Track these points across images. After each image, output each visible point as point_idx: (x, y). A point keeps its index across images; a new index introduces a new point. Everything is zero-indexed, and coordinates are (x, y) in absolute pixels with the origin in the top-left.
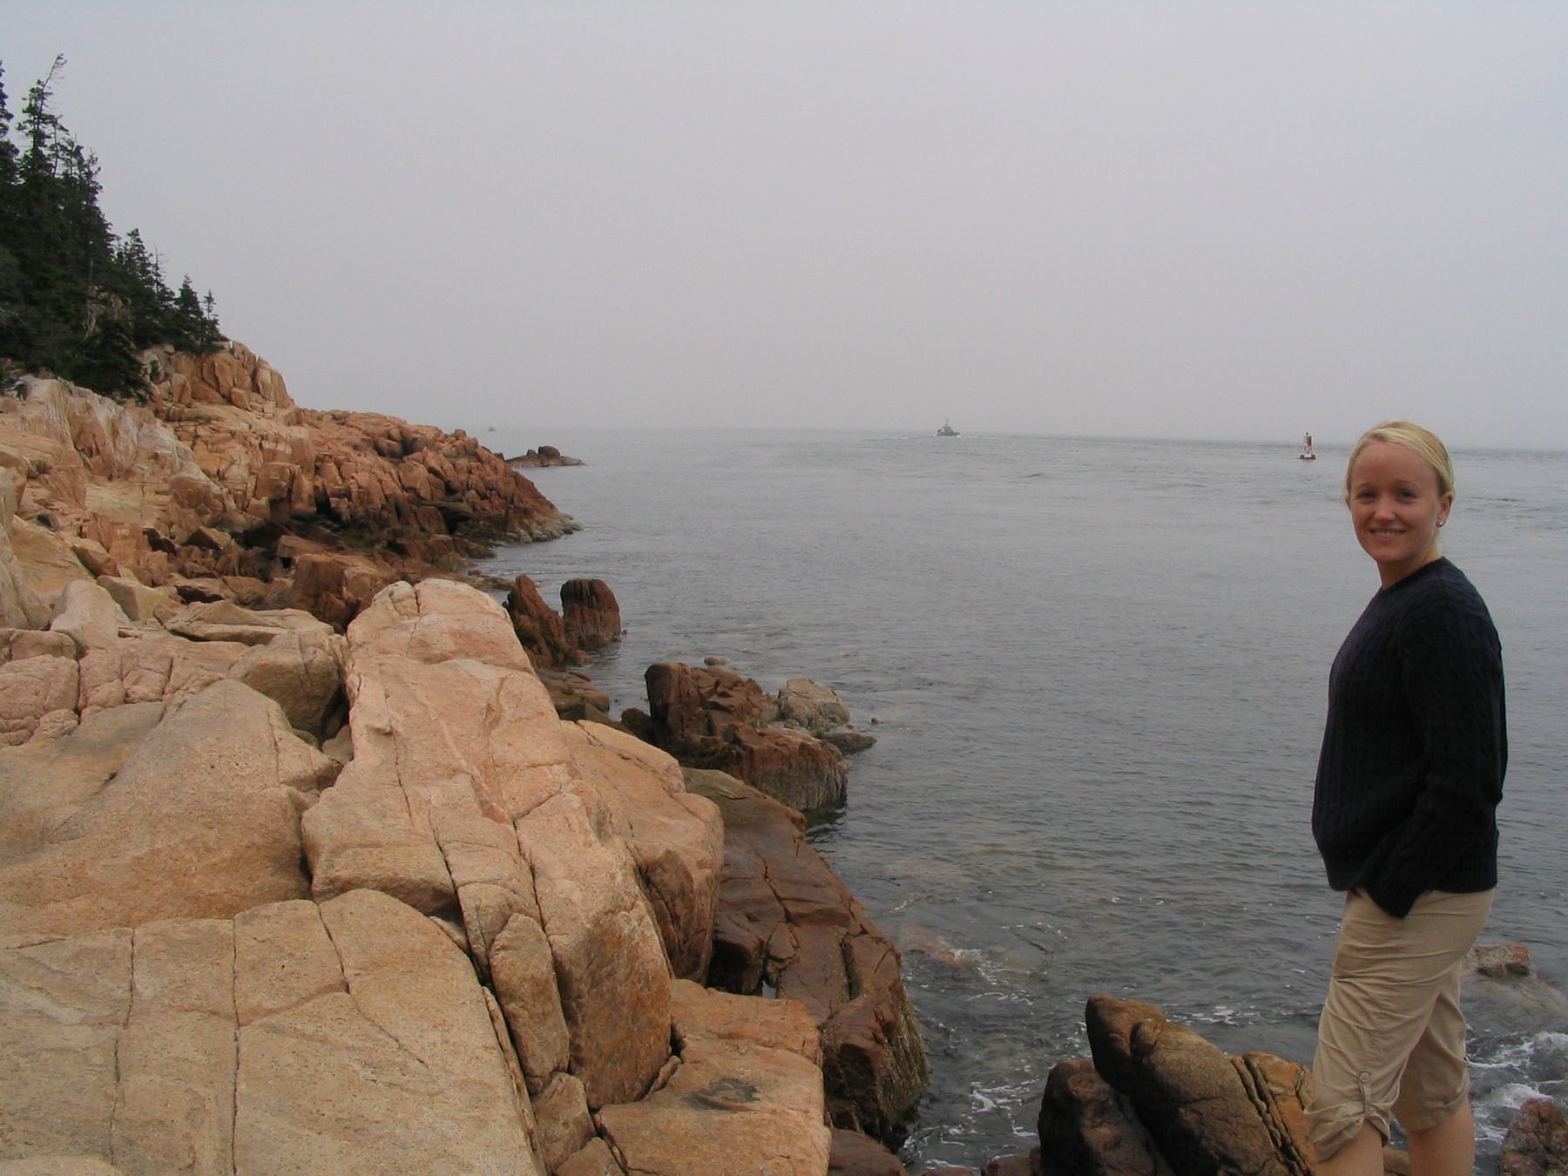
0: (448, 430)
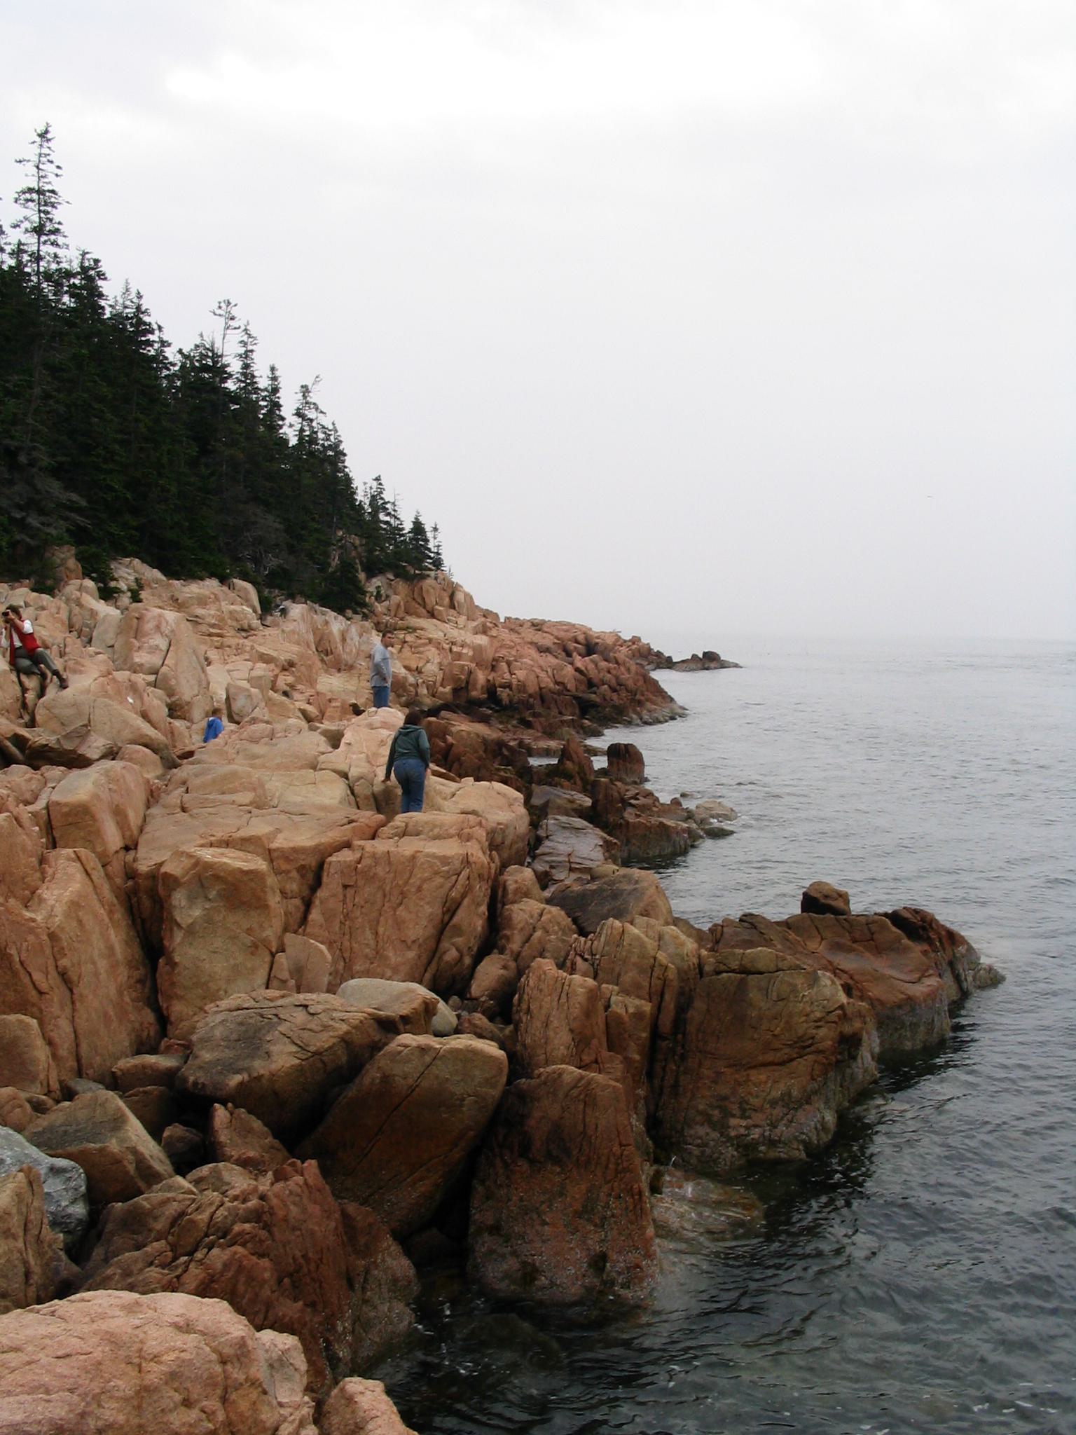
0: (627, 636)
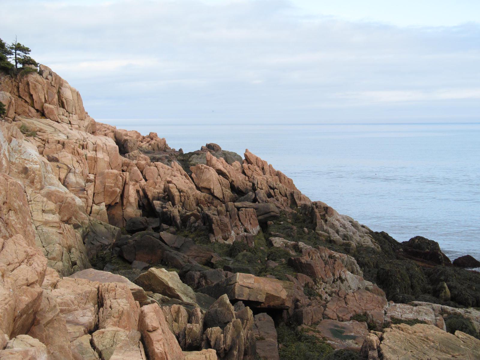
0: (145, 133)
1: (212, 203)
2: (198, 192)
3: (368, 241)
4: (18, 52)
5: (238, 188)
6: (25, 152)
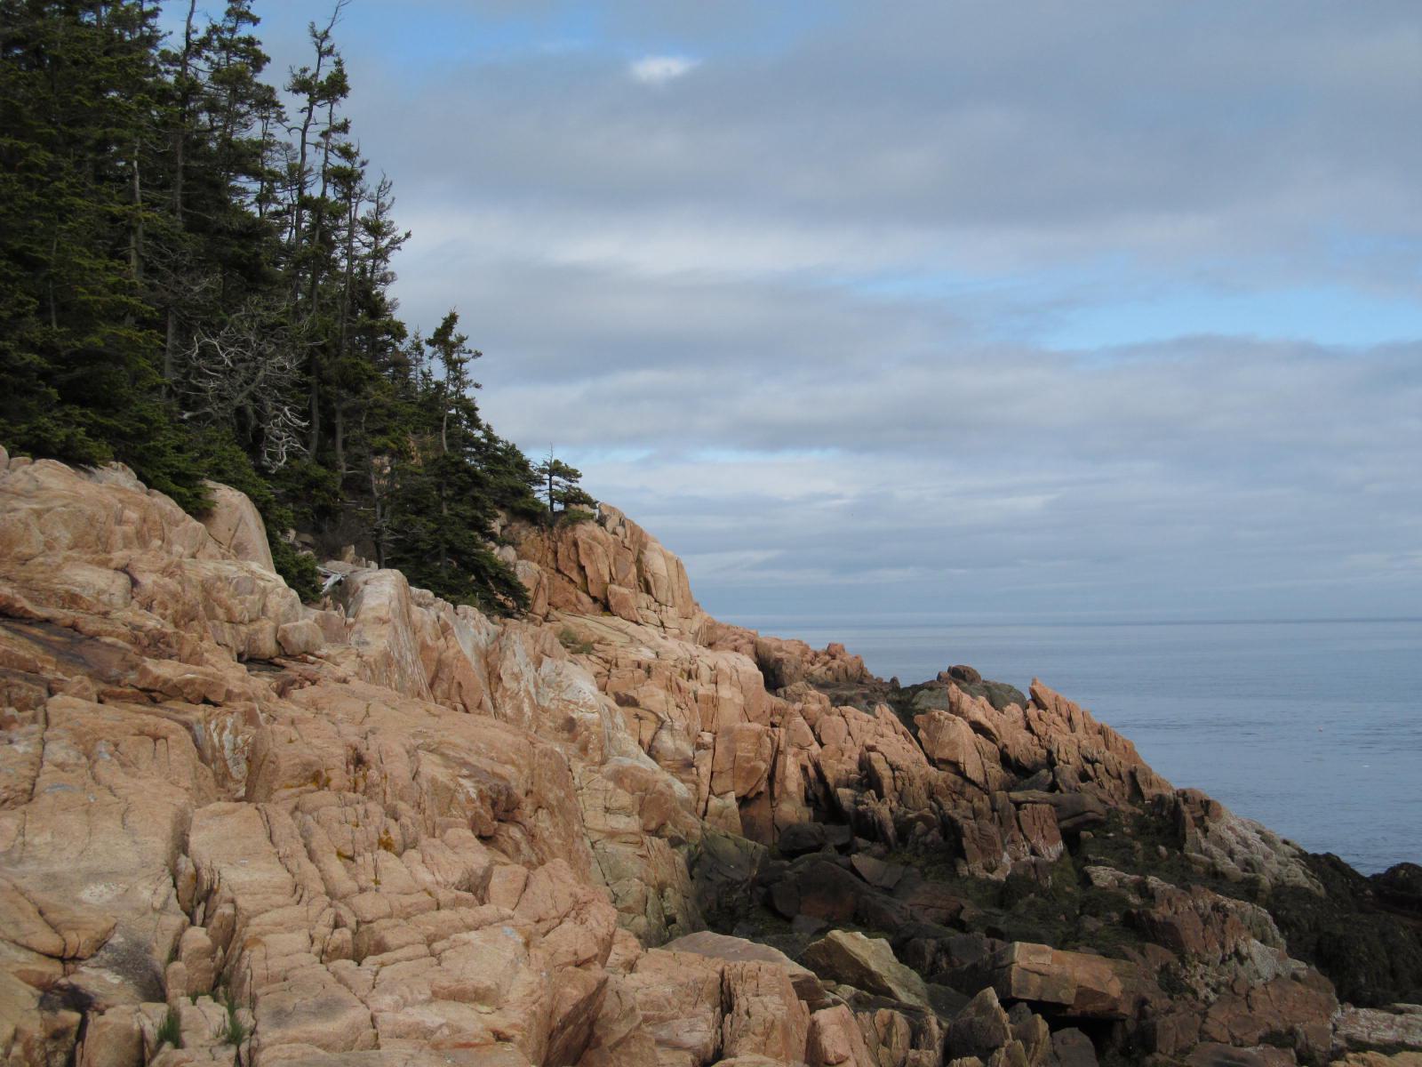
0: (819, 646)
1: (961, 794)
2: (932, 769)
3: (1298, 875)
4: (555, 478)
5: (1017, 760)
6: (569, 686)
